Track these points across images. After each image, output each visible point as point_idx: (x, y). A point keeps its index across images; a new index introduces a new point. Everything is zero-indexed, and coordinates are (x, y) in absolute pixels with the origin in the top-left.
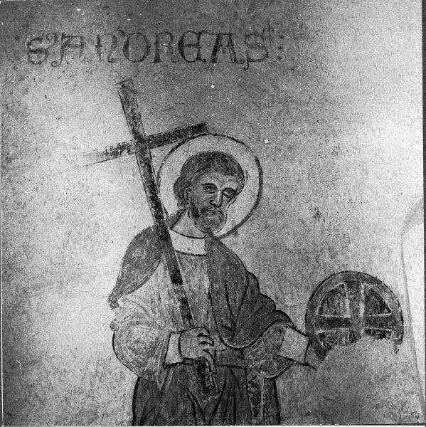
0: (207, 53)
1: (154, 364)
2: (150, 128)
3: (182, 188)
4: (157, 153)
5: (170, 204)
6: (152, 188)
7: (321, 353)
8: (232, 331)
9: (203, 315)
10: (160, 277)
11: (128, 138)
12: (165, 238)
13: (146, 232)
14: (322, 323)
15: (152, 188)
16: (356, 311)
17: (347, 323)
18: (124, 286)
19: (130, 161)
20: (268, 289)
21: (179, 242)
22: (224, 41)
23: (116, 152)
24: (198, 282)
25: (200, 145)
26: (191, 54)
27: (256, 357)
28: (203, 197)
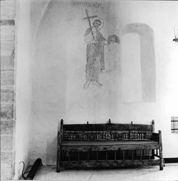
0: (97, 6)
1: (89, 43)
2: (90, 16)
3: (94, 23)
4: (91, 19)
5: (92, 25)
6: (90, 23)
7: (109, 44)
8: (99, 40)
9: (95, 37)
10: (90, 34)
11: (87, 17)
12: (91, 29)
13: (89, 29)
14: (109, 40)
15: (90, 23)
16: (114, 39)
17: (113, 41)
18: (86, 35)
19: (87, 20)
20: (103, 36)
21: (93, 30)
22: (100, 4)
23: (85, 18)
24: (95, 35)
25: (96, 18)
26: (95, 6)
27: (102, 44)
28: (96, 25)
